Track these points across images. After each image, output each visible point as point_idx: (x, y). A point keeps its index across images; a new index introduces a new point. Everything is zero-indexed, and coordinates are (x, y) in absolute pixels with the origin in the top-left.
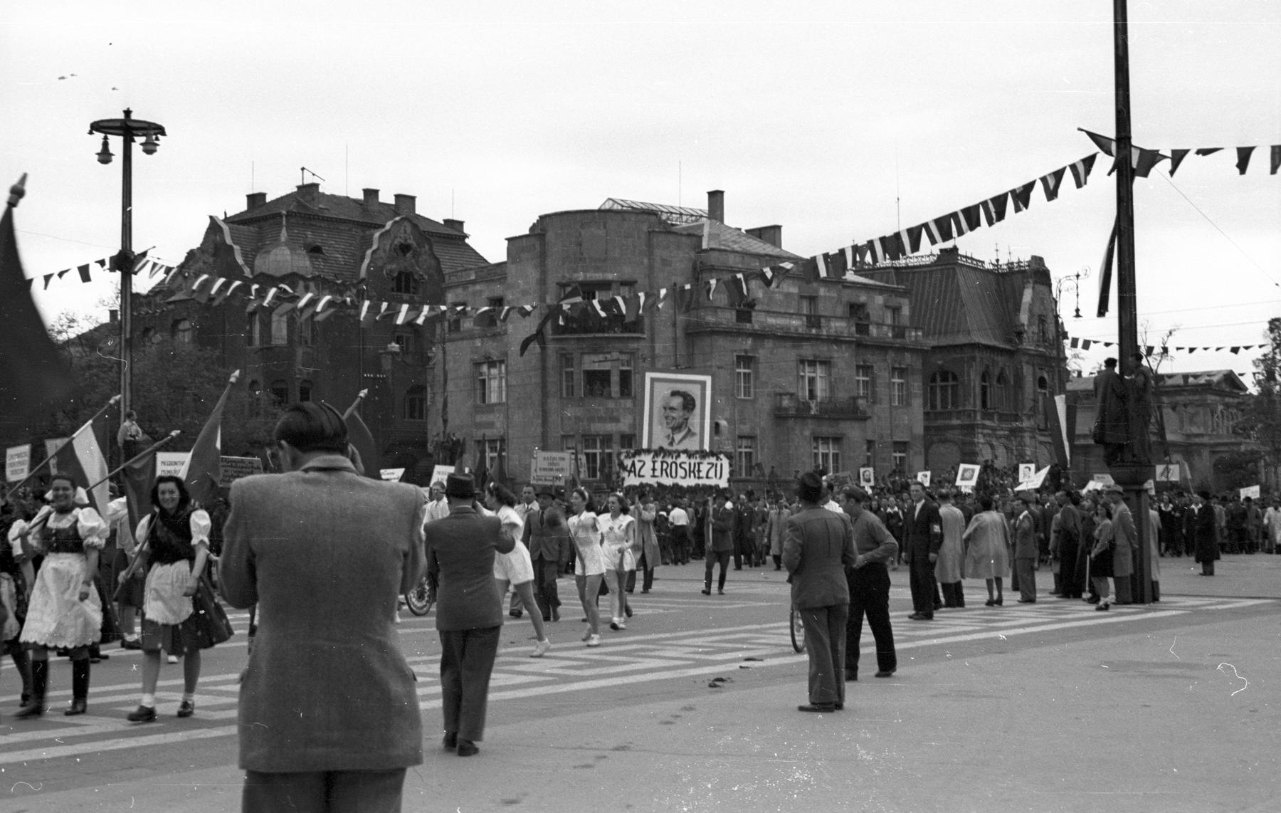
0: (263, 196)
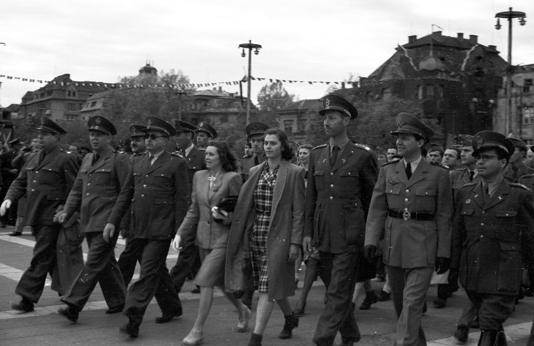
0: (415, 36)
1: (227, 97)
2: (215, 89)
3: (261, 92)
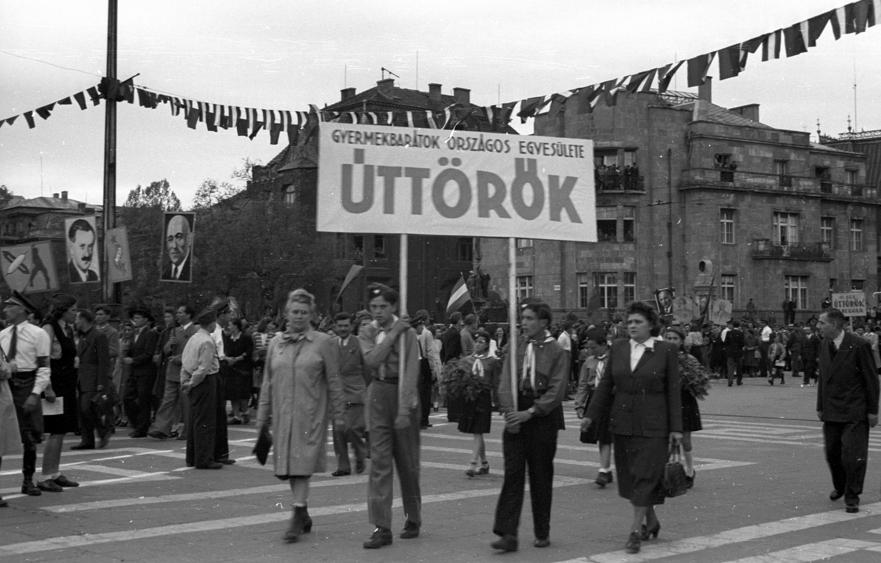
0: (353, 90)
1: (75, 210)
2: (56, 195)
3: (130, 198)
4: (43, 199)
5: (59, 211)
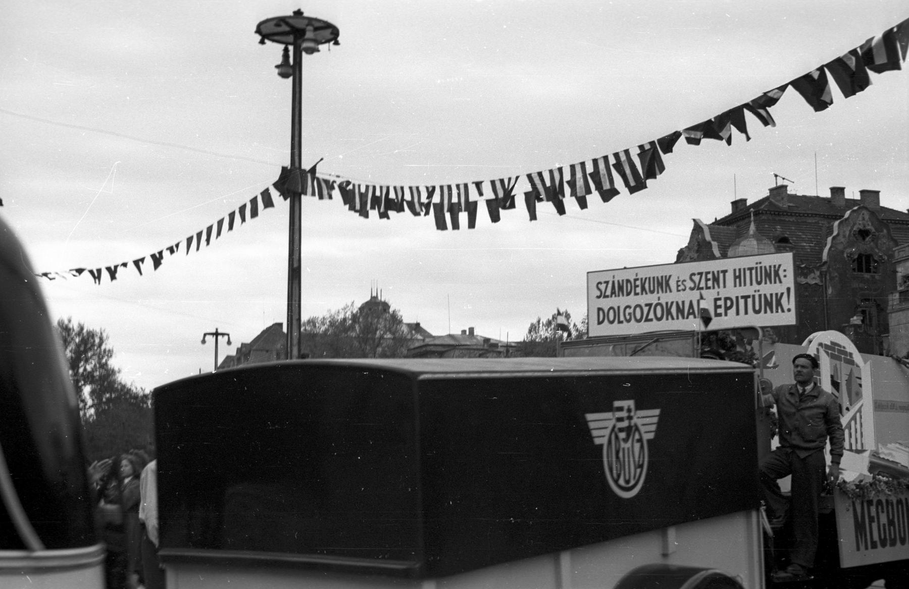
0: (745, 201)
2: (464, 332)
3: (530, 331)
4: (451, 336)
5: (464, 347)
